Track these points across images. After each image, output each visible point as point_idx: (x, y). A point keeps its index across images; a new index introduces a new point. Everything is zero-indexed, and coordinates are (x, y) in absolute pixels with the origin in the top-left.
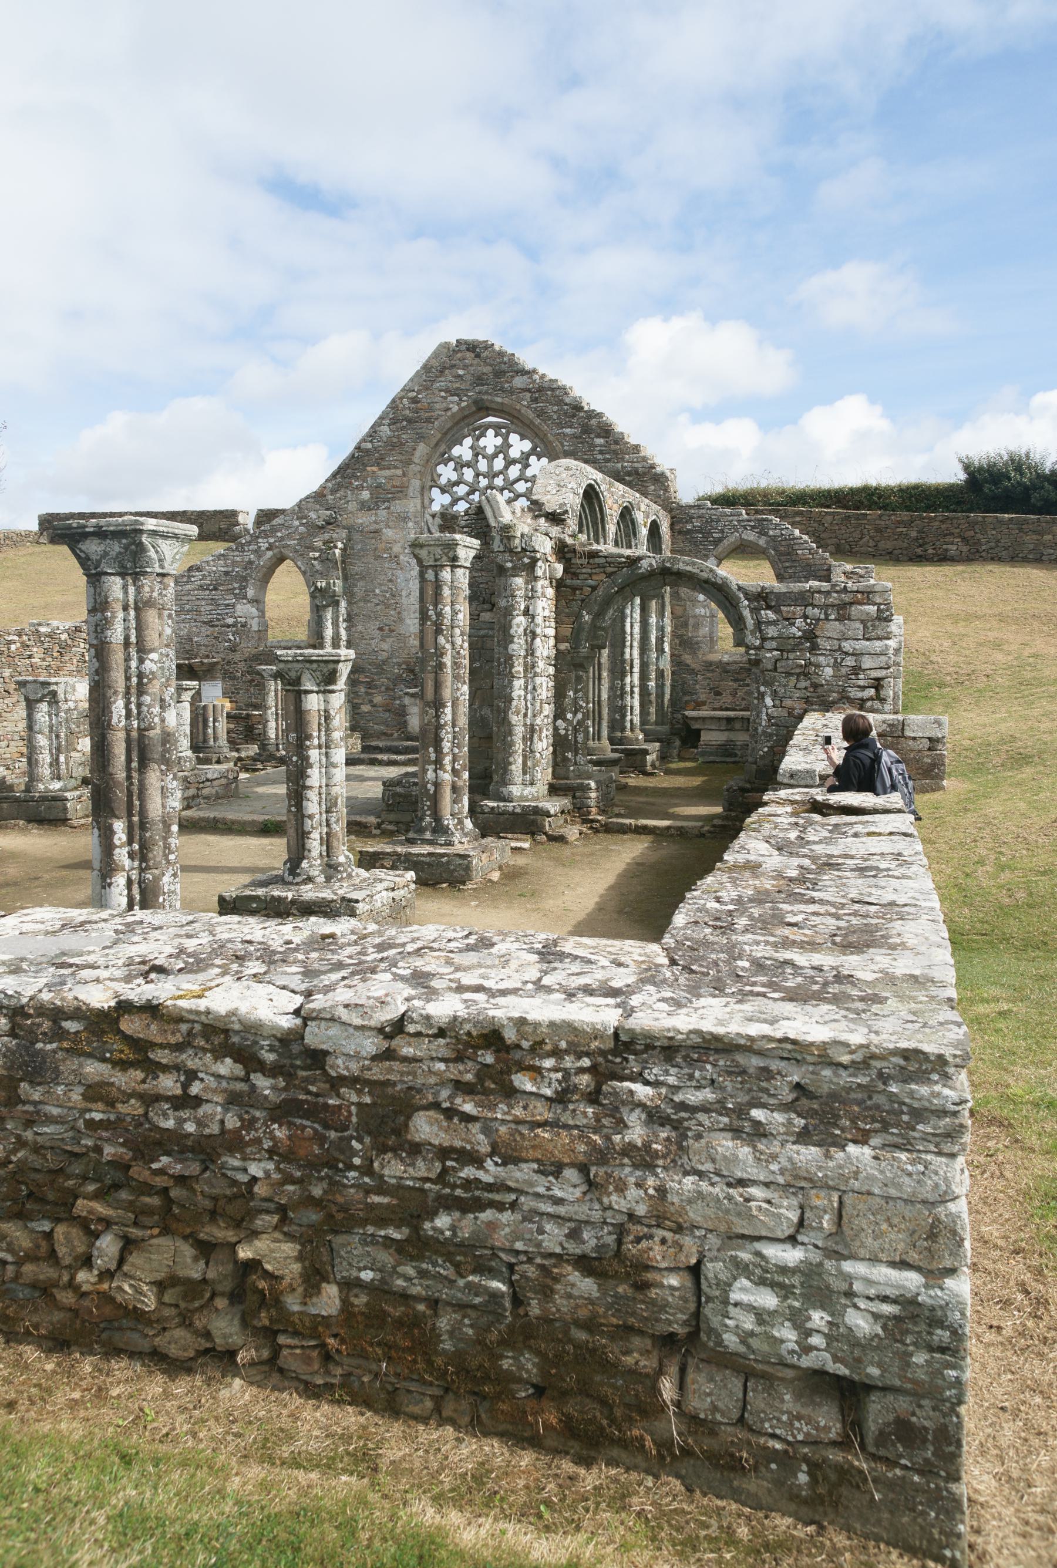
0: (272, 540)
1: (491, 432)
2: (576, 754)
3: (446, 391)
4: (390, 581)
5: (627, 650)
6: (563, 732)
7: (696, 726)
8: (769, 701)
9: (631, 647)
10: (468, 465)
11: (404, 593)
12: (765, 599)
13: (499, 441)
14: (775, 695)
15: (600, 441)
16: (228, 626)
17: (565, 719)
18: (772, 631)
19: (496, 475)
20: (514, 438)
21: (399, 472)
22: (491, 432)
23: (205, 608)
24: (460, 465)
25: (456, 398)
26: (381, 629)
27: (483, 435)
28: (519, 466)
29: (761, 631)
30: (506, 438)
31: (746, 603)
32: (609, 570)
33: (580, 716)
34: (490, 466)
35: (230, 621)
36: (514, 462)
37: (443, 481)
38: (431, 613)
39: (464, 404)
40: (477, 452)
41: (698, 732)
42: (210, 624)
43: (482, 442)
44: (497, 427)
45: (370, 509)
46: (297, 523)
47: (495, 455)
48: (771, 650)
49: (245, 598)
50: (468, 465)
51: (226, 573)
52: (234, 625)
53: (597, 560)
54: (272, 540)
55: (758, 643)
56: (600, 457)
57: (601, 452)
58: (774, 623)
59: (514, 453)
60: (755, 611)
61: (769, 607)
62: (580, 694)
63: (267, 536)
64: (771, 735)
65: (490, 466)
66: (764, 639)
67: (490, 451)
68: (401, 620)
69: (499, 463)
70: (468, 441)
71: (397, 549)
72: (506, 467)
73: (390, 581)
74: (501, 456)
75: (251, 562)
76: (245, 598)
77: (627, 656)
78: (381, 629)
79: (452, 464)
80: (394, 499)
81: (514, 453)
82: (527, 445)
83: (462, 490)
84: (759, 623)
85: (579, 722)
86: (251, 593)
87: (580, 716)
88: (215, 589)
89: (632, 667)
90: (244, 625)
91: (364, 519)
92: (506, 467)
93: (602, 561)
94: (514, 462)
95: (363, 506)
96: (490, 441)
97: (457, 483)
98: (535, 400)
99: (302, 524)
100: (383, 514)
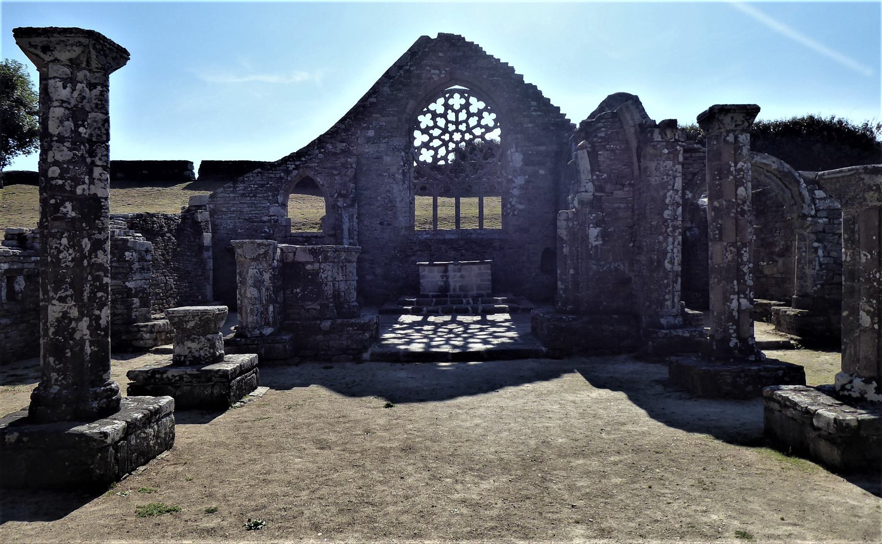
0: (297, 163)
1: (457, 96)
3: (430, 66)
4: (388, 191)
8: (820, 252)
10: (441, 116)
11: (398, 200)
13: (463, 101)
14: (825, 248)
15: (534, 103)
16: (265, 222)
18: (821, 205)
19: (461, 123)
20: (473, 100)
21: (396, 119)
22: (457, 96)
23: (246, 209)
24: (435, 116)
25: (437, 72)
26: (381, 223)
27: (451, 97)
28: (476, 118)
29: (815, 205)
30: (467, 99)
31: (804, 185)
34: (457, 117)
35: (265, 218)
36: (473, 115)
37: (423, 126)
38: (732, 169)
39: (443, 76)
40: (447, 106)
42: (250, 220)
43: (451, 102)
44: (462, 93)
45: (374, 143)
46: (317, 151)
47: (460, 110)
48: (822, 218)
49: (277, 202)
50: (441, 116)
51: (262, 186)
52: (269, 221)
53: (697, 154)
54: (297, 163)
55: (813, 212)
56: (534, 113)
57: (535, 110)
58: (824, 199)
59: (473, 109)
60: (811, 192)
61: (820, 189)
63: (294, 161)
64: (822, 276)
65: (457, 117)
66: (817, 210)
67: (457, 107)
68: (395, 217)
69: (441, 122)
70: (441, 101)
71: (393, 169)
72: (468, 118)
74: (464, 111)
75: (281, 178)
76: (277, 202)
78: (381, 223)
79: (429, 116)
80: (392, 136)
81: (473, 109)
82: (482, 105)
83: (436, 132)
84: (813, 200)
86: (280, 199)
88: (255, 196)
90: (276, 221)
91: (369, 149)
92: (468, 118)
94: (473, 115)
95: (369, 140)
96: (457, 101)
97: (433, 128)
98: (493, 75)
99: (320, 152)
100: (383, 147)
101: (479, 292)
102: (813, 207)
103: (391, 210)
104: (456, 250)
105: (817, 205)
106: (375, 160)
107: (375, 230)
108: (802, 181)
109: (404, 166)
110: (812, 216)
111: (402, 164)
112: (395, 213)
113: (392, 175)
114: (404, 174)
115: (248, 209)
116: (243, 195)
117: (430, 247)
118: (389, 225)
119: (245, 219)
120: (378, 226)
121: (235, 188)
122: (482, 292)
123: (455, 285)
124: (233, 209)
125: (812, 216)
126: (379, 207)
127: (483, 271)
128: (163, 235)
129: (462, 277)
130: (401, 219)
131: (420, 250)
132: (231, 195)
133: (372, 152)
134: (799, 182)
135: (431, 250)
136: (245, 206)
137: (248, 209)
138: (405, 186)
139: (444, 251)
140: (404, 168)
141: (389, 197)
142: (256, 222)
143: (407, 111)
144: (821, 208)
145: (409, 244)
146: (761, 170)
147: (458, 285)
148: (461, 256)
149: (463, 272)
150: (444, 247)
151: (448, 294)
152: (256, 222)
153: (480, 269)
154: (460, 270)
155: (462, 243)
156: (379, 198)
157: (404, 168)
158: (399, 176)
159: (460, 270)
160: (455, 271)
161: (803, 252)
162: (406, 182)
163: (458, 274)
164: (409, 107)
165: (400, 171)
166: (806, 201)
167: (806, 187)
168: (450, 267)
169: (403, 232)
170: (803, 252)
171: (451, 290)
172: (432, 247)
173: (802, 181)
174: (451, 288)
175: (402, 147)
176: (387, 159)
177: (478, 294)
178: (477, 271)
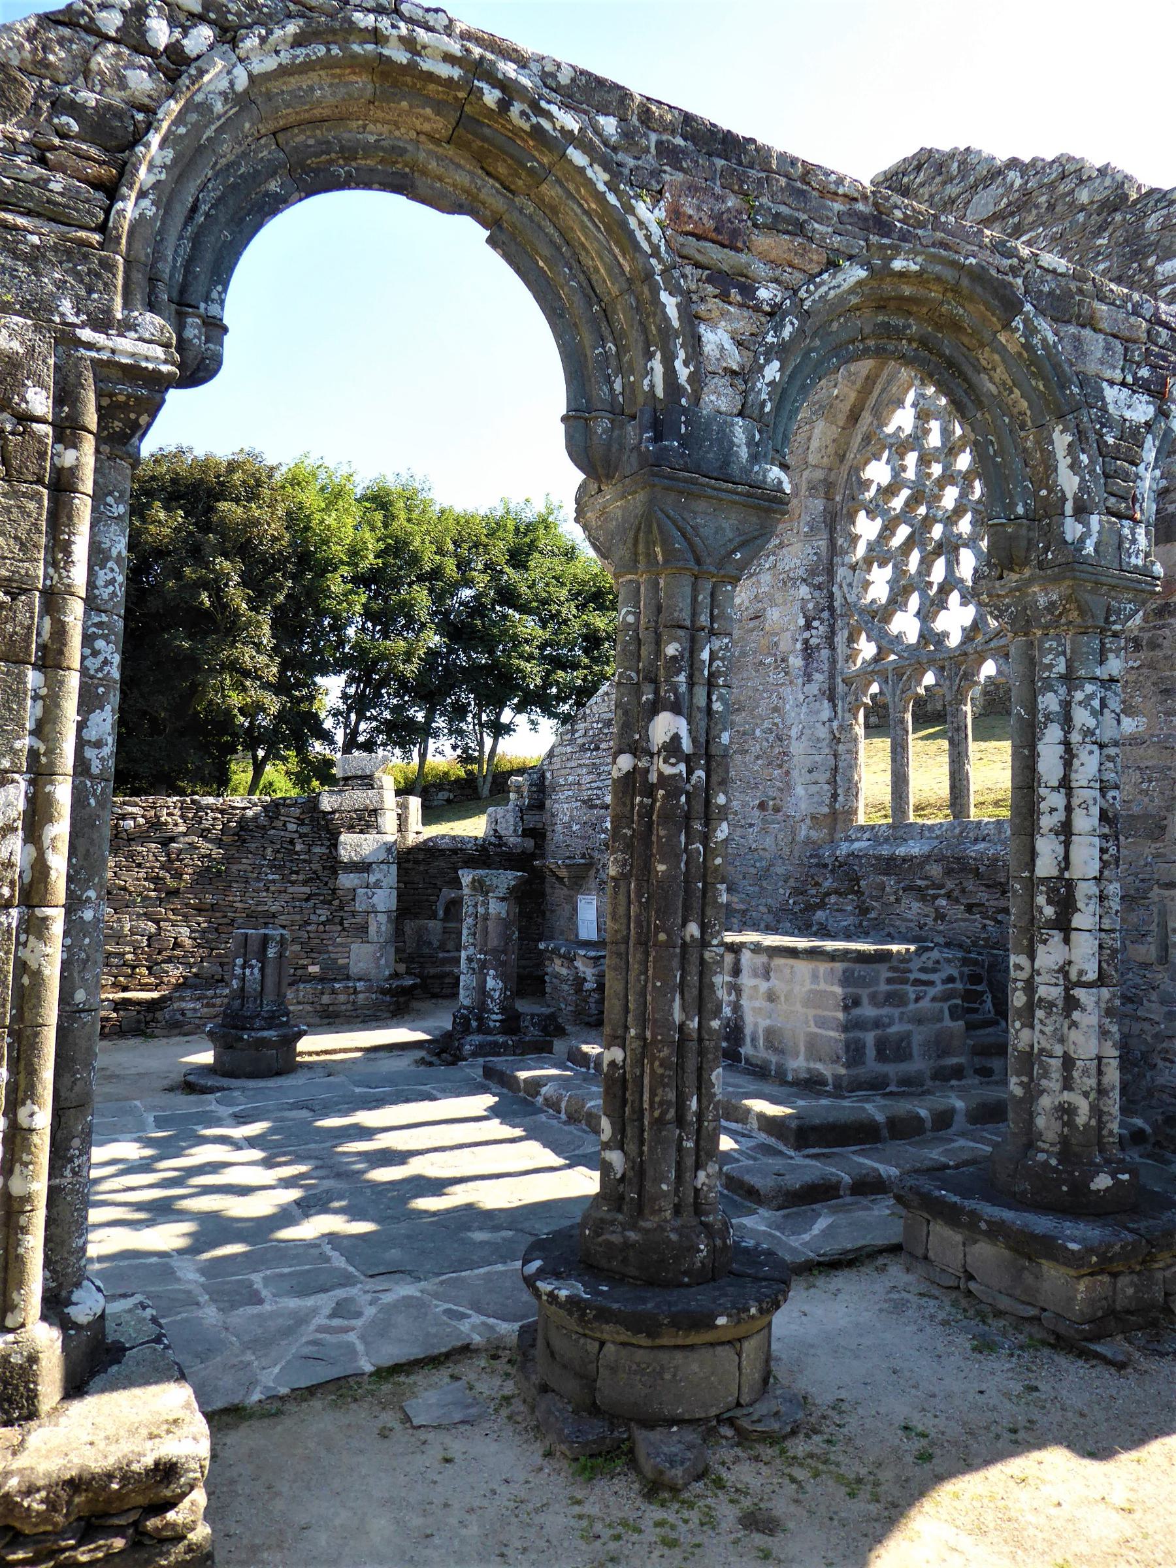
4: (776, 709)
11: (794, 732)
68: (788, 787)
71: (785, 644)
73: (776, 709)
77: (1045, 867)
78: (762, 806)
88: (597, 748)
101: (812, 1065)
103: (780, 766)
104: (921, 894)
106: (752, 624)
107: (751, 825)
109: (808, 626)
111: (802, 622)
112: (787, 773)
113: (783, 660)
114: (808, 651)
115: (588, 778)
116: (583, 749)
117: (857, 880)
118: (777, 810)
119: (584, 802)
120: (756, 812)
121: (573, 732)
122: (819, 1066)
123: (756, 1025)
124: (571, 778)
126: (757, 758)
127: (823, 986)
128: (166, 842)
129: (771, 997)
130: (800, 791)
131: (837, 892)
132: (569, 749)
133: (747, 604)
135: (859, 893)
136: (584, 771)
137: (588, 778)
138: (813, 689)
139: (892, 899)
140: (806, 635)
141: (776, 724)
142: (595, 807)
143: (812, 459)
145: (813, 870)
147: (764, 1023)
148: (935, 920)
149: (775, 982)
150: (890, 882)
151: (742, 1051)
152: (595, 807)
153: (815, 977)
154: (766, 974)
155: (935, 870)
156: (758, 732)
157: (806, 635)
158: (796, 662)
159: (766, 974)
160: (755, 975)
162: (817, 676)
163: (764, 986)
164: (815, 444)
165: (799, 646)
168: (746, 956)
169: (803, 833)
171: (748, 1040)
172: (862, 883)
174: (748, 1031)
175: (801, 572)
176: (774, 615)
177: (809, 1070)
178: (808, 986)
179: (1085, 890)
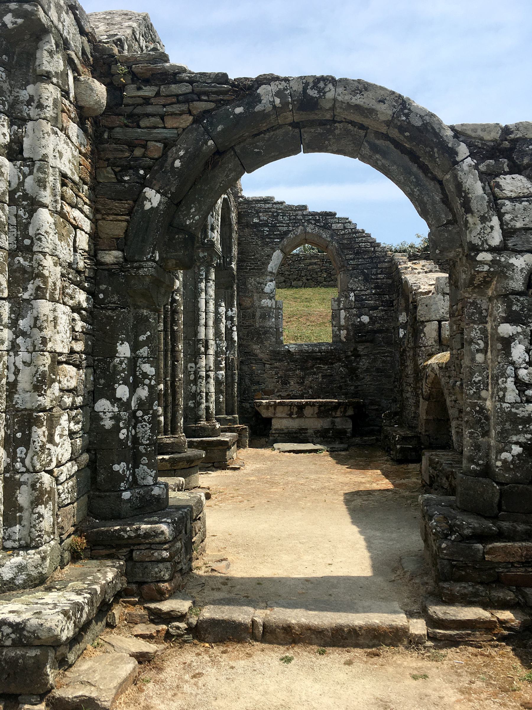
2: (136, 465)
5: (202, 329)
6: (108, 424)
7: (265, 414)
9: (206, 325)
12: (507, 153)
17: (114, 400)
29: (500, 216)
32: (201, 106)
33: (143, 393)
41: (268, 421)
53: (174, 88)
55: (496, 239)
62: (144, 351)
77: (202, 336)
85: (141, 404)
87: (143, 393)
89: (207, 348)
93: (185, 88)
102: (495, 221)
105: (507, 217)
108: (463, 150)
110: (492, 250)
125: (492, 250)
134: (453, 153)
144: (519, 225)
146: (362, 133)
161: (478, 351)
166: (474, 205)
167: (476, 167)
170: (478, 351)
173: (463, 150)
179: (212, 342)
